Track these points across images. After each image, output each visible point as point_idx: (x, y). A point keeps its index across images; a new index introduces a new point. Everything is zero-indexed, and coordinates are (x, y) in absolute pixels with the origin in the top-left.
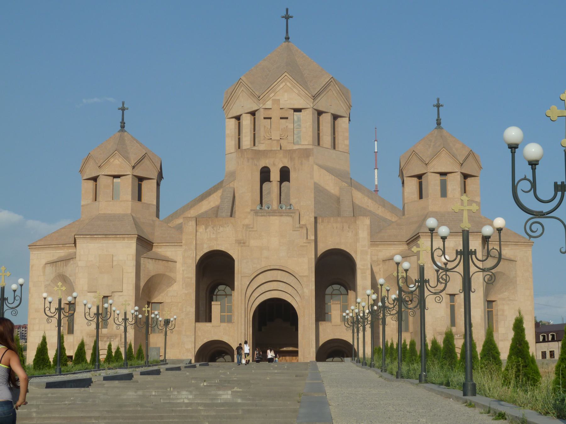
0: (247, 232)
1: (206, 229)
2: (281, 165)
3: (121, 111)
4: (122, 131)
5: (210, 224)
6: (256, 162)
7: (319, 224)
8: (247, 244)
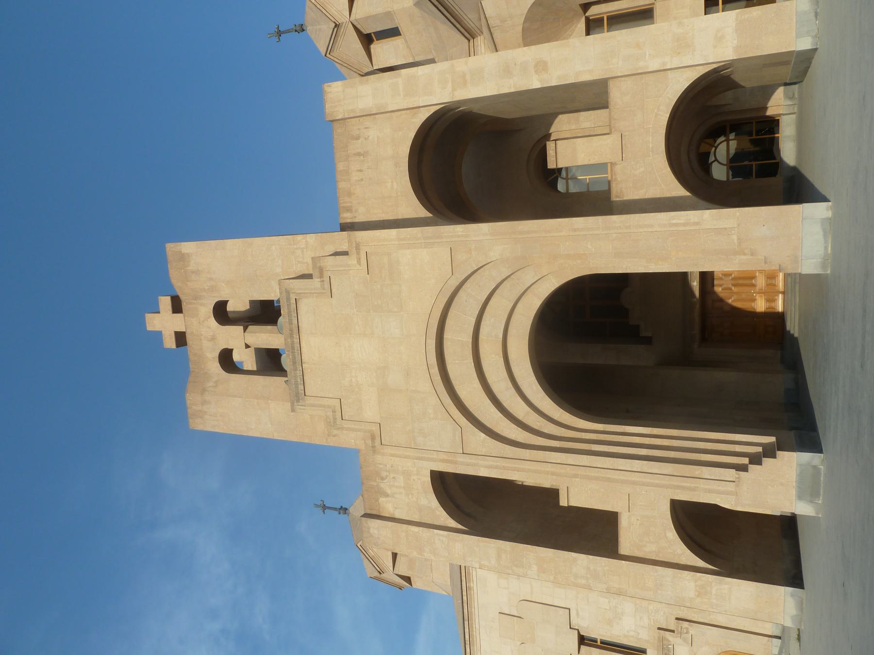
0: (345, 426)
1: (387, 495)
2: (213, 322)
3: (326, 511)
4: (348, 514)
5: (375, 484)
6: (211, 384)
7: (355, 217)
8: (374, 429)
